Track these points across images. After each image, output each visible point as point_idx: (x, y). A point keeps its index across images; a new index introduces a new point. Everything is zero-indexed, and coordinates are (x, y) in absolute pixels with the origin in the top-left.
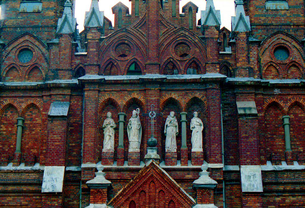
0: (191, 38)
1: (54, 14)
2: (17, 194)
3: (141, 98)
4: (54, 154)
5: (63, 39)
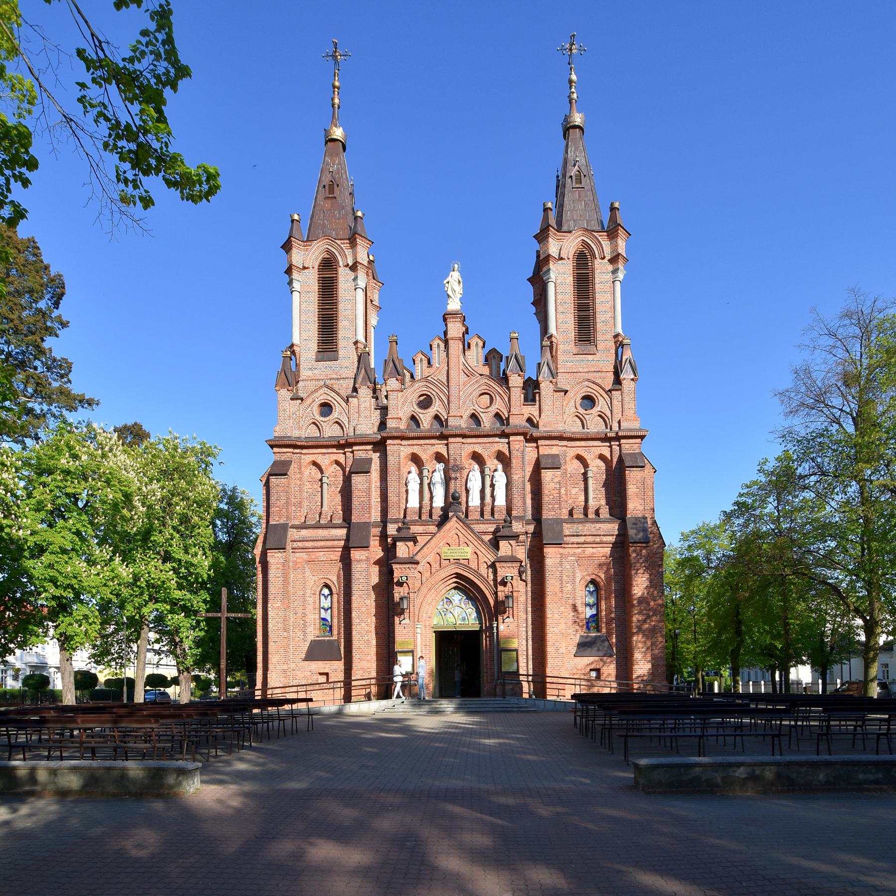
2: (326, 550)
3: (443, 450)
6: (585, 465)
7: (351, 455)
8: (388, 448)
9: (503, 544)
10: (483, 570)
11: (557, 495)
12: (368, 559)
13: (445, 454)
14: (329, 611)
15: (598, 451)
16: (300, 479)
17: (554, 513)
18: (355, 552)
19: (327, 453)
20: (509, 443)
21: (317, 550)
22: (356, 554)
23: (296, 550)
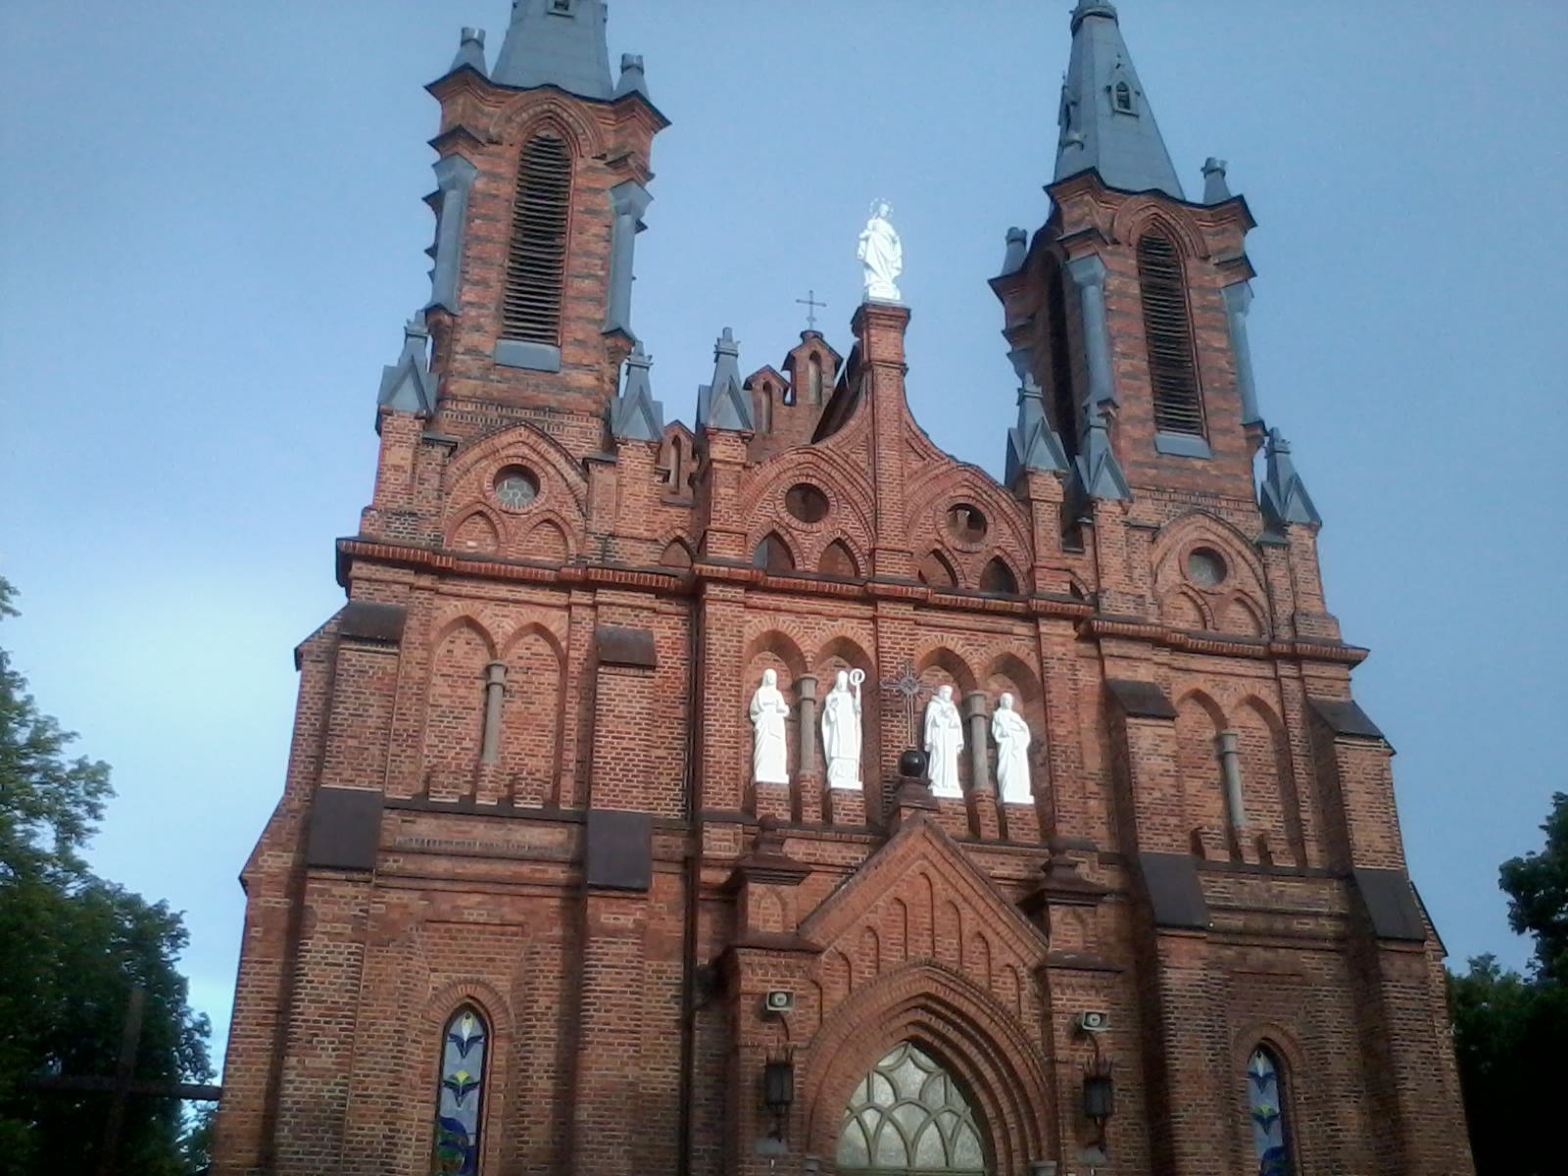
0: (990, 496)
1: (596, 383)
2: (489, 888)
3: (859, 633)
4: (617, 775)
5: (630, 453)
6: (1221, 721)
7: (588, 614)
8: (709, 608)
9: (1056, 914)
10: (1006, 990)
11: (1173, 791)
12: (640, 929)
13: (867, 645)
14: (474, 1094)
15: (1247, 687)
16: (425, 665)
17: (1166, 840)
18: (602, 903)
19: (517, 602)
20: (1037, 637)
21: (459, 887)
22: (605, 913)
23: (392, 882)
